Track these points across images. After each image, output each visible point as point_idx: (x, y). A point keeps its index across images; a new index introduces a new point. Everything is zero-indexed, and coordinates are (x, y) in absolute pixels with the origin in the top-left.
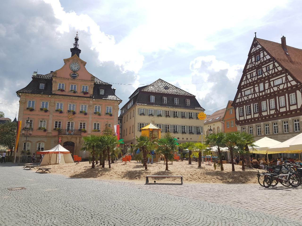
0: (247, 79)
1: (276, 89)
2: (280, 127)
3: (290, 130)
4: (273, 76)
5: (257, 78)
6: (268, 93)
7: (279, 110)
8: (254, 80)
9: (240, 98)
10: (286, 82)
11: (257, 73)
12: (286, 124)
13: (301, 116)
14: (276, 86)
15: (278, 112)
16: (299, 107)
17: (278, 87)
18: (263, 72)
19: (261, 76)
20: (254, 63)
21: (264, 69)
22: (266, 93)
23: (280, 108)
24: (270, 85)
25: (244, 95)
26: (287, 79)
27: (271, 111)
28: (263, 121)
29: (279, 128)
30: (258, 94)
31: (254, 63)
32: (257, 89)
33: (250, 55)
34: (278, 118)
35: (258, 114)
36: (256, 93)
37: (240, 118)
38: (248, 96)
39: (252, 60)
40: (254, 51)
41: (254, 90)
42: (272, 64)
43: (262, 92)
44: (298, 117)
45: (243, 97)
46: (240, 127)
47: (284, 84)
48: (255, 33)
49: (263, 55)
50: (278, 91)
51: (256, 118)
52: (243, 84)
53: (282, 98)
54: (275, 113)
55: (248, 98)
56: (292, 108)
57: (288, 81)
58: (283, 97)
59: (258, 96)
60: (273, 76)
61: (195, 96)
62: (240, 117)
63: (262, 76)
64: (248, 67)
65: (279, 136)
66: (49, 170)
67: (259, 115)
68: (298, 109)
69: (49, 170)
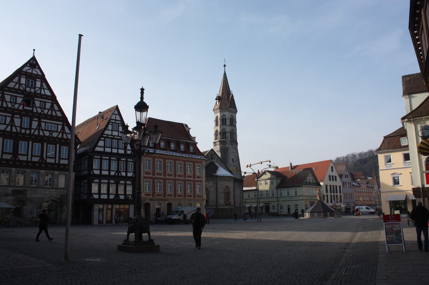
1: (47, 134)
4: (46, 117)
10: (61, 132)
14: (49, 131)
15: (44, 161)
17: (51, 132)
18: (34, 106)
19: (31, 109)
21: (37, 104)
22: (32, 133)
24: (39, 125)
27: (4, 155)
28: (14, 166)
29: (40, 180)
30: (19, 129)
31: (24, 86)
32: (17, 122)
33: (19, 73)
34: (40, 168)
35: (12, 156)
36: (16, 127)
40: (28, 71)
41: (12, 121)
43: (26, 129)
47: (60, 133)
50: (48, 137)
53: (51, 147)
54: (40, 161)
57: (64, 132)
59: (19, 131)
60: (46, 117)
63: (33, 109)
65: (38, 189)
66: (43, 231)
69: (43, 231)
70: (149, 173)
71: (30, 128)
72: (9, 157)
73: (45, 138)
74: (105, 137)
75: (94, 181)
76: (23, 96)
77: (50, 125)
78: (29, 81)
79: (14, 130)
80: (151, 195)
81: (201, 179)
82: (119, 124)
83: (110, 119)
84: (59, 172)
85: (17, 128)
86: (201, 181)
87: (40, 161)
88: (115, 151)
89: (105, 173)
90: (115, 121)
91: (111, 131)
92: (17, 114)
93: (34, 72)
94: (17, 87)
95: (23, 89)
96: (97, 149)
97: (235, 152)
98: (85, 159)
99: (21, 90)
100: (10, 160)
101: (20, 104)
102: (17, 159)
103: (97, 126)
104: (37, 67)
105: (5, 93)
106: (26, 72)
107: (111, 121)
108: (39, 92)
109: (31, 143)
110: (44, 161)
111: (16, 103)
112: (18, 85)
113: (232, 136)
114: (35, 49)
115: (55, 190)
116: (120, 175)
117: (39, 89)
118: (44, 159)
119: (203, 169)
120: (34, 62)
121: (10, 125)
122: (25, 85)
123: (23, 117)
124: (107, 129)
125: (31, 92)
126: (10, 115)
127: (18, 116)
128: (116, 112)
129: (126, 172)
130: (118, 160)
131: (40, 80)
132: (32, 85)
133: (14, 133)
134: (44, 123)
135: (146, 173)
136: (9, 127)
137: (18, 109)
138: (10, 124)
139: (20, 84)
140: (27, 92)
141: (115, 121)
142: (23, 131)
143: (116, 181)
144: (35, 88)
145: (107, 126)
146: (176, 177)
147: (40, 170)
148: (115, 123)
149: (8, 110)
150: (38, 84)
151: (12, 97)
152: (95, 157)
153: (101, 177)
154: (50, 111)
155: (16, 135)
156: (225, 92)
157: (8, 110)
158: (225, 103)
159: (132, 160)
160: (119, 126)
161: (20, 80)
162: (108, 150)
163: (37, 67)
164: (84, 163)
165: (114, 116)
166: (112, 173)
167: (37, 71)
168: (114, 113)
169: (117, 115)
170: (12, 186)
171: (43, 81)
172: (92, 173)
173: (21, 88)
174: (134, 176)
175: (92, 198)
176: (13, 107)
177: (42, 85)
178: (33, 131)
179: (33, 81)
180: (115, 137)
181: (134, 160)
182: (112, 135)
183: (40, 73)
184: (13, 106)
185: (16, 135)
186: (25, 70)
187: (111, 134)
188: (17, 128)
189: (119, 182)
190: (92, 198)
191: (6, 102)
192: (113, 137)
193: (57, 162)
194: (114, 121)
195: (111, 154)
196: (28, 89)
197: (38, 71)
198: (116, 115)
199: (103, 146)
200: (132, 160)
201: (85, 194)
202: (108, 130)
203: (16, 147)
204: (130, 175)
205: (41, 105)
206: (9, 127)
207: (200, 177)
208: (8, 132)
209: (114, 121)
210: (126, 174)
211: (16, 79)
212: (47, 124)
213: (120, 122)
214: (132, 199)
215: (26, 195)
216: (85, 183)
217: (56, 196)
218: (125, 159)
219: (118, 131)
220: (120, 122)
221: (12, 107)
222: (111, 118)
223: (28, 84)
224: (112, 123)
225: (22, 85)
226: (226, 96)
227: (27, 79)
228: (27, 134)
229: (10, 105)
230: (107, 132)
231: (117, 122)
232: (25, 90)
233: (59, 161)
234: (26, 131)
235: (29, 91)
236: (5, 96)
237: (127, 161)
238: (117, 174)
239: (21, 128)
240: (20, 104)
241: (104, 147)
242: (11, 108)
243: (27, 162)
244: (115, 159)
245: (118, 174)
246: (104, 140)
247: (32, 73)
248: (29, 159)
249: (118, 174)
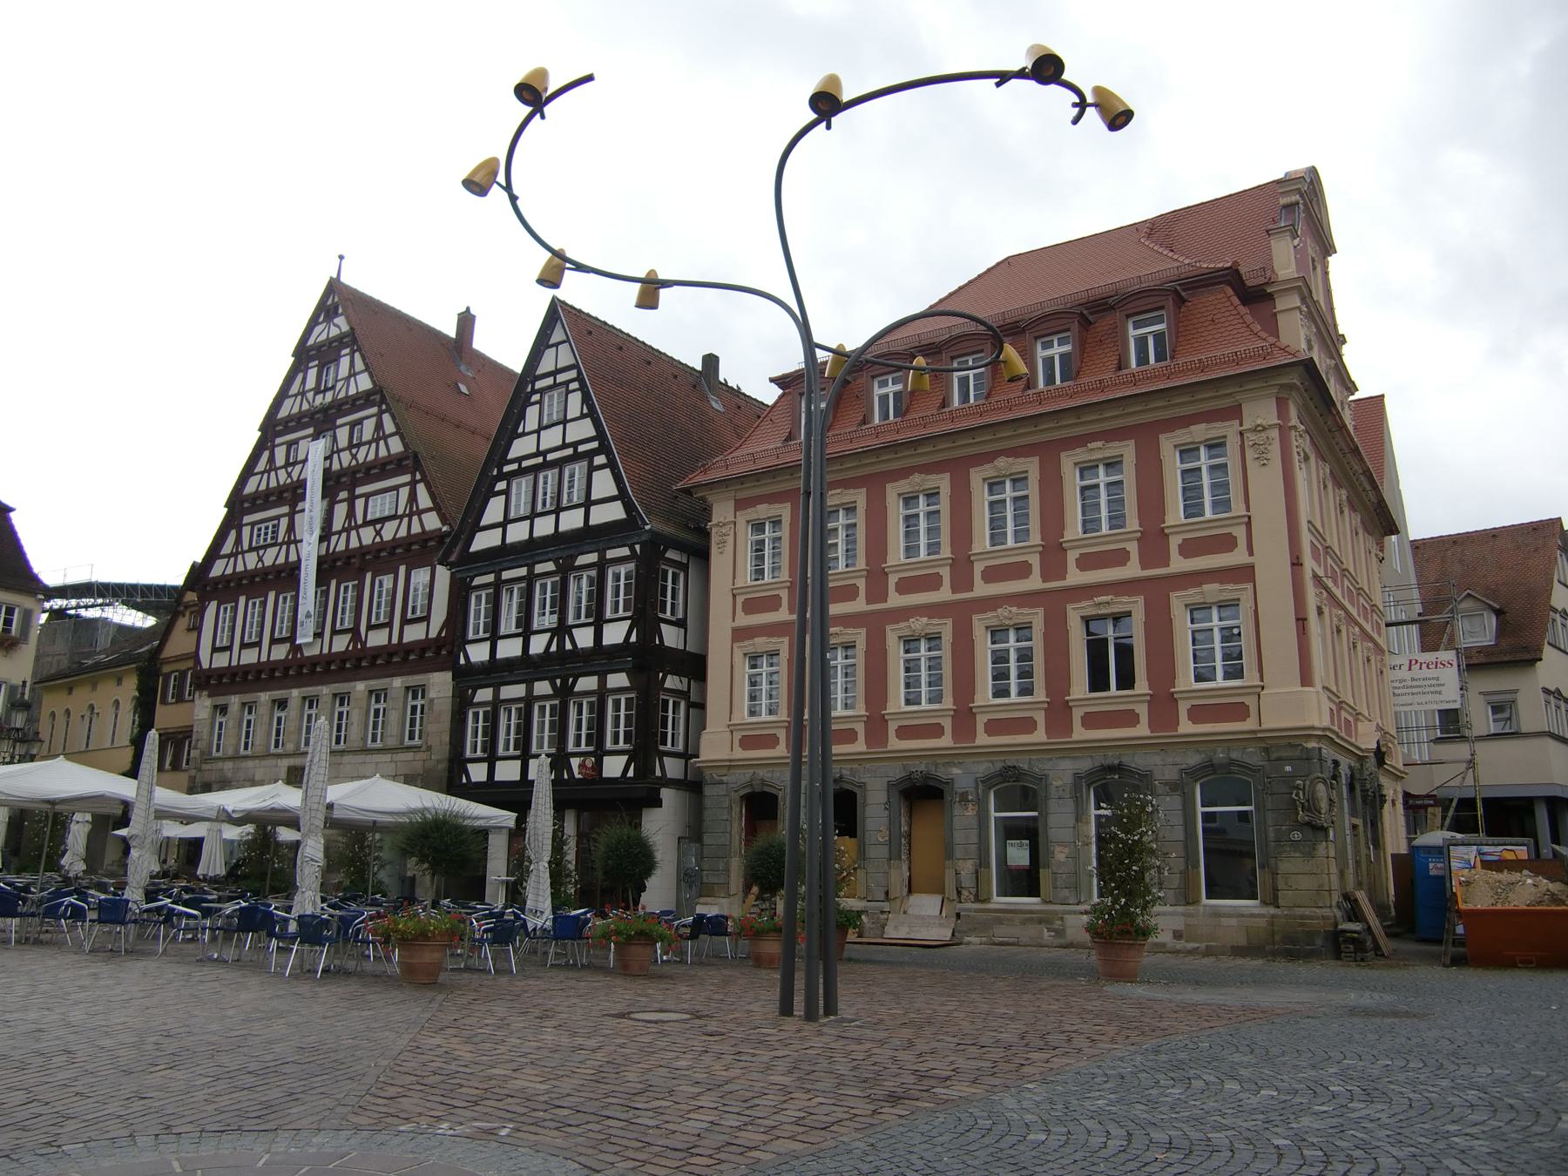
2: (356, 716)
6: (337, 550)
8: (295, 479)
9: (228, 556)
12: (419, 702)
20: (310, 395)
23: (370, 627)
24: (351, 514)
25: (246, 547)
26: (413, 498)
31: (310, 395)
33: (304, 354)
38: (261, 552)
39: (304, 381)
42: (374, 419)
45: (243, 553)
47: (401, 517)
48: (341, 257)
49: (350, 370)
52: (250, 488)
61: (12, 510)
62: (215, 650)
64: (283, 413)
81: (1238, 557)
89: (509, 649)
116: (568, 646)
129: (599, 625)
143: (558, 682)
159: (625, 551)
175: (464, 780)
190: (464, 780)
200: (625, 551)
204: (615, 634)
210: (598, 636)
214: (631, 774)
230: (521, 447)
238: (553, 648)
245: (561, 644)
249: (561, 644)
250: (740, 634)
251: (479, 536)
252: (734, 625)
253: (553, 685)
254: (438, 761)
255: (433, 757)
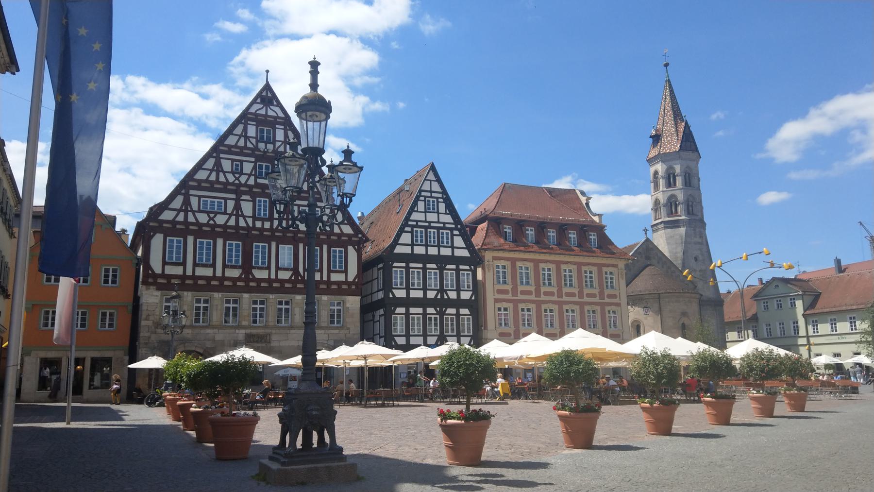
0: (218, 168)
3: (322, 321)
5: (255, 180)
7: (302, 274)
11: (254, 168)
13: (349, 297)
15: (300, 278)
16: (351, 278)
22: (274, 227)
28: (248, 290)
30: (250, 221)
31: (254, 141)
32: (247, 208)
35: (241, 271)
36: (244, 217)
37: (167, 267)
40: (258, 112)
41: (238, 207)
44: (344, 297)
46: (158, 293)
51: (335, 283)
52: (202, 175)
54: (293, 278)
55: (212, 219)
56: (335, 277)
58: (287, 247)
59: (251, 225)
62: (165, 263)
65: (292, 331)
67: (241, 274)
68: (346, 282)
70: (505, 292)
71: (271, 219)
72: (235, 273)
73: (299, 235)
74: (412, 227)
75: (396, 312)
76: (253, 159)
77: (209, 202)
78: (262, 131)
79: (242, 223)
80: (513, 335)
82: (437, 198)
83: (420, 191)
84: (330, 296)
85: (247, 218)
86: (618, 305)
87: (293, 278)
88: (433, 251)
89: (416, 294)
90: (431, 194)
91: (424, 214)
92: (245, 193)
93: (270, 113)
94: (241, 143)
95: (252, 146)
96: (399, 250)
97: (700, 241)
98: (379, 269)
99: (249, 149)
100: (239, 279)
101: (250, 175)
102: (251, 277)
103: (400, 205)
104: (275, 103)
105: (222, 156)
106: (255, 114)
107: (423, 194)
108: (281, 149)
109: (274, 244)
110: (300, 278)
111: (241, 173)
112: (242, 139)
113: (691, 208)
114: (269, 70)
115: (323, 332)
116: (446, 297)
117: (281, 145)
118: (301, 276)
119: (620, 279)
120: (269, 95)
121: (234, 215)
122: (256, 138)
123: (257, 199)
124: (416, 209)
125: (267, 150)
126: (234, 196)
127: (248, 197)
128: (431, 176)
130: (441, 269)
131: (282, 127)
132: (269, 138)
133: (243, 228)
134: (197, 198)
135: (500, 292)
136: (233, 218)
137: (246, 185)
138: (235, 213)
139: (247, 138)
140: (259, 150)
141: (431, 194)
142: (259, 224)
143: (438, 309)
144: (274, 142)
145: (415, 203)
146: (562, 298)
147: (294, 295)
148: (431, 197)
149: (229, 187)
150: (280, 135)
151: (235, 163)
152: (395, 264)
153: (408, 302)
154: (214, 174)
155: (246, 232)
156: (669, 119)
157: (229, 187)
158: (671, 143)
160: (438, 202)
161: (245, 130)
162: (420, 250)
163: (275, 103)
164: (378, 278)
165: (427, 183)
166: (431, 295)
167: (276, 111)
168: (427, 178)
169: (433, 181)
170: (245, 327)
171: (288, 128)
172: (391, 296)
173: (249, 145)
174: (473, 298)
175: (393, 344)
176: (237, 182)
177: (286, 136)
178: (276, 223)
179: (270, 130)
180: (432, 225)
181: (472, 267)
182: (425, 221)
183: (281, 115)
184: (237, 179)
185: (246, 232)
186: (252, 110)
187: (424, 220)
188: (247, 218)
189: (446, 310)
191: (224, 173)
192: (427, 224)
193: (325, 278)
194: (429, 194)
195: (425, 259)
196: (261, 146)
197: (277, 109)
198: (432, 182)
199: (410, 243)
200: (467, 267)
201: (381, 337)
202: (417, 211)
203: (247, 255)
204: (466, 295)
205: (234, 167)
206: (233, 218)
207: (614, 296)
208: (231, 227)
209: (429, 194)
210: (459, 295)
211: (239, 130)
212: (202, 199)
213: (440, 195)
215: (270, 342)
216: (380, 316)
217: (326, 342)
218: (454, 267)
219: (438, 213)
220: (440, 195)
221: (235, 181)
222: (422, 189)
223: (262, 137)
224: (425, 197)
225: (251, 139)
226: (673, 127)
227: (259, 128)
228: (267, 230)
229: (231, 178)
230: (415, 216)
231: (434, 195)
232: (256, 148)
233: (329, 276)
234: (263, 225)
235: (264, 148)
236: (222, 161)
237: (458, 271)
238: (439, 297)
239: (255, 218)
240: (250, 175)
241: (412, 245)
242: (233, 184)
243: (269, 280)
244: (434, 266)
245: (442, 296)
246: (411, 232)
247: (266, 115)
248: (273, 276)
249: (442, 296)
250: (496, 301)
251: (398, 247)
252: (494, 297)
253: (436, 310)
254: (354, 334)
255: (351, 333)
